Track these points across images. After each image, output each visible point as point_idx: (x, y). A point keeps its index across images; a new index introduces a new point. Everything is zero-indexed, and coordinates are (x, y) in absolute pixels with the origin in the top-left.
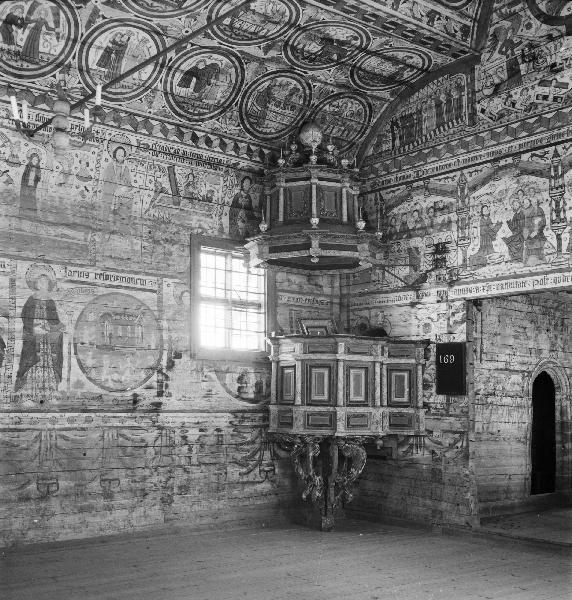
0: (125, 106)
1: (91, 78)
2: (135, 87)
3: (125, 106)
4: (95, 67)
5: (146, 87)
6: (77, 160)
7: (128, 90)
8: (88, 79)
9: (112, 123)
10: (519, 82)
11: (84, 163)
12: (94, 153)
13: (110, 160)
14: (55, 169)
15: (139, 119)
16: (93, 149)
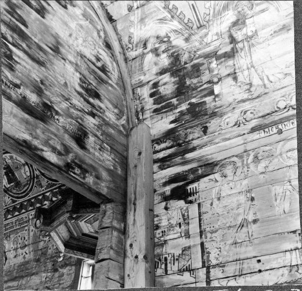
0: (31, 195)
1: (11, 192)
2: (29, 182)
3: (31, 195)
4: (9, 186)
5: (32, 178)
6: (20, 238)
7: (27, 186)
8: (11, 193)
9: (31, 208)
10: (78, 39)
11: (23, 238)
12: (26, 230)
13: (34, 229)
14: (11, 249)
15: (40, 197)
16: (26, 228)
